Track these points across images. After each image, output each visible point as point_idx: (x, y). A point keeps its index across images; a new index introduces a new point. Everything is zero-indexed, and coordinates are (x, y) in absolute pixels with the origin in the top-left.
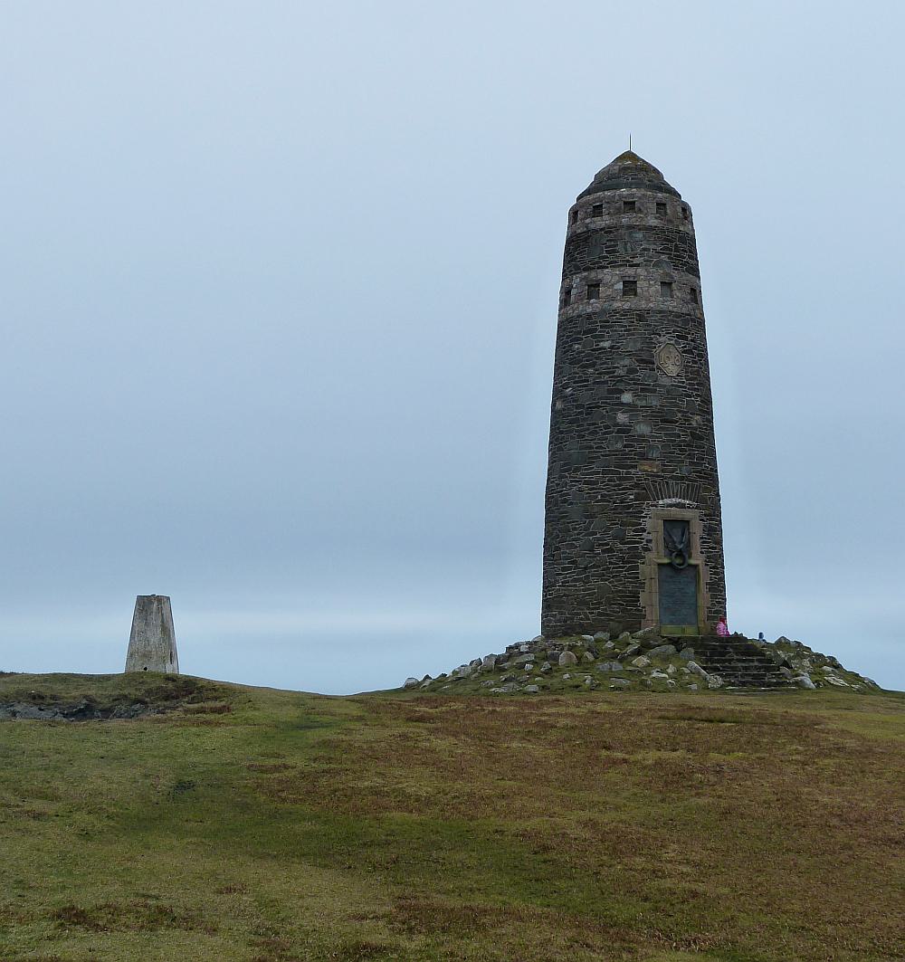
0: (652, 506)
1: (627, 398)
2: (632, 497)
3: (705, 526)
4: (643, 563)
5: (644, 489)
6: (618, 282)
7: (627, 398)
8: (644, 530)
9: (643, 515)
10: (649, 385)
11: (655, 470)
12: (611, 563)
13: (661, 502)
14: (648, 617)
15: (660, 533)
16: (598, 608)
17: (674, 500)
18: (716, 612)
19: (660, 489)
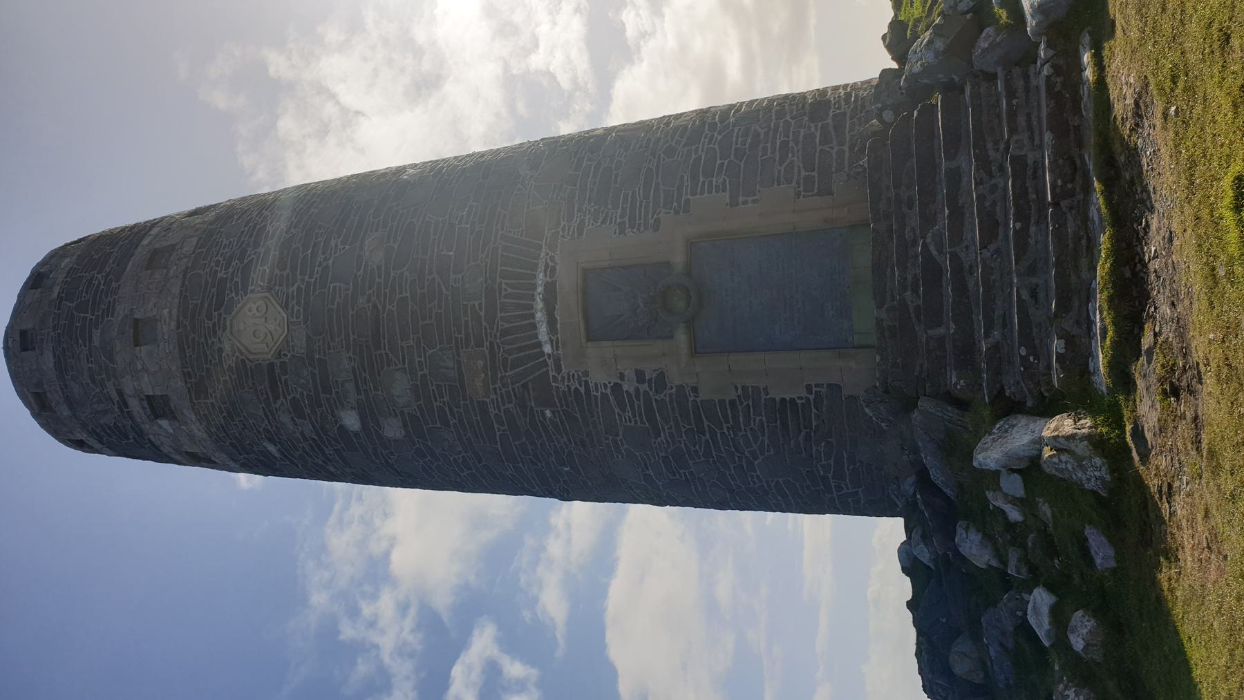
0: (559, 369)
1: (351, 421)
2: (548, 413)
4: (695, 390)
5: (525, 386)
6: (160, 427)
7: (351, 421)
8: (617, 388)
9: (582, 390)
10: (313, 375)
11: (480, 363)
13: (547, 349)
17: (539, 315)
19: (520, 349)
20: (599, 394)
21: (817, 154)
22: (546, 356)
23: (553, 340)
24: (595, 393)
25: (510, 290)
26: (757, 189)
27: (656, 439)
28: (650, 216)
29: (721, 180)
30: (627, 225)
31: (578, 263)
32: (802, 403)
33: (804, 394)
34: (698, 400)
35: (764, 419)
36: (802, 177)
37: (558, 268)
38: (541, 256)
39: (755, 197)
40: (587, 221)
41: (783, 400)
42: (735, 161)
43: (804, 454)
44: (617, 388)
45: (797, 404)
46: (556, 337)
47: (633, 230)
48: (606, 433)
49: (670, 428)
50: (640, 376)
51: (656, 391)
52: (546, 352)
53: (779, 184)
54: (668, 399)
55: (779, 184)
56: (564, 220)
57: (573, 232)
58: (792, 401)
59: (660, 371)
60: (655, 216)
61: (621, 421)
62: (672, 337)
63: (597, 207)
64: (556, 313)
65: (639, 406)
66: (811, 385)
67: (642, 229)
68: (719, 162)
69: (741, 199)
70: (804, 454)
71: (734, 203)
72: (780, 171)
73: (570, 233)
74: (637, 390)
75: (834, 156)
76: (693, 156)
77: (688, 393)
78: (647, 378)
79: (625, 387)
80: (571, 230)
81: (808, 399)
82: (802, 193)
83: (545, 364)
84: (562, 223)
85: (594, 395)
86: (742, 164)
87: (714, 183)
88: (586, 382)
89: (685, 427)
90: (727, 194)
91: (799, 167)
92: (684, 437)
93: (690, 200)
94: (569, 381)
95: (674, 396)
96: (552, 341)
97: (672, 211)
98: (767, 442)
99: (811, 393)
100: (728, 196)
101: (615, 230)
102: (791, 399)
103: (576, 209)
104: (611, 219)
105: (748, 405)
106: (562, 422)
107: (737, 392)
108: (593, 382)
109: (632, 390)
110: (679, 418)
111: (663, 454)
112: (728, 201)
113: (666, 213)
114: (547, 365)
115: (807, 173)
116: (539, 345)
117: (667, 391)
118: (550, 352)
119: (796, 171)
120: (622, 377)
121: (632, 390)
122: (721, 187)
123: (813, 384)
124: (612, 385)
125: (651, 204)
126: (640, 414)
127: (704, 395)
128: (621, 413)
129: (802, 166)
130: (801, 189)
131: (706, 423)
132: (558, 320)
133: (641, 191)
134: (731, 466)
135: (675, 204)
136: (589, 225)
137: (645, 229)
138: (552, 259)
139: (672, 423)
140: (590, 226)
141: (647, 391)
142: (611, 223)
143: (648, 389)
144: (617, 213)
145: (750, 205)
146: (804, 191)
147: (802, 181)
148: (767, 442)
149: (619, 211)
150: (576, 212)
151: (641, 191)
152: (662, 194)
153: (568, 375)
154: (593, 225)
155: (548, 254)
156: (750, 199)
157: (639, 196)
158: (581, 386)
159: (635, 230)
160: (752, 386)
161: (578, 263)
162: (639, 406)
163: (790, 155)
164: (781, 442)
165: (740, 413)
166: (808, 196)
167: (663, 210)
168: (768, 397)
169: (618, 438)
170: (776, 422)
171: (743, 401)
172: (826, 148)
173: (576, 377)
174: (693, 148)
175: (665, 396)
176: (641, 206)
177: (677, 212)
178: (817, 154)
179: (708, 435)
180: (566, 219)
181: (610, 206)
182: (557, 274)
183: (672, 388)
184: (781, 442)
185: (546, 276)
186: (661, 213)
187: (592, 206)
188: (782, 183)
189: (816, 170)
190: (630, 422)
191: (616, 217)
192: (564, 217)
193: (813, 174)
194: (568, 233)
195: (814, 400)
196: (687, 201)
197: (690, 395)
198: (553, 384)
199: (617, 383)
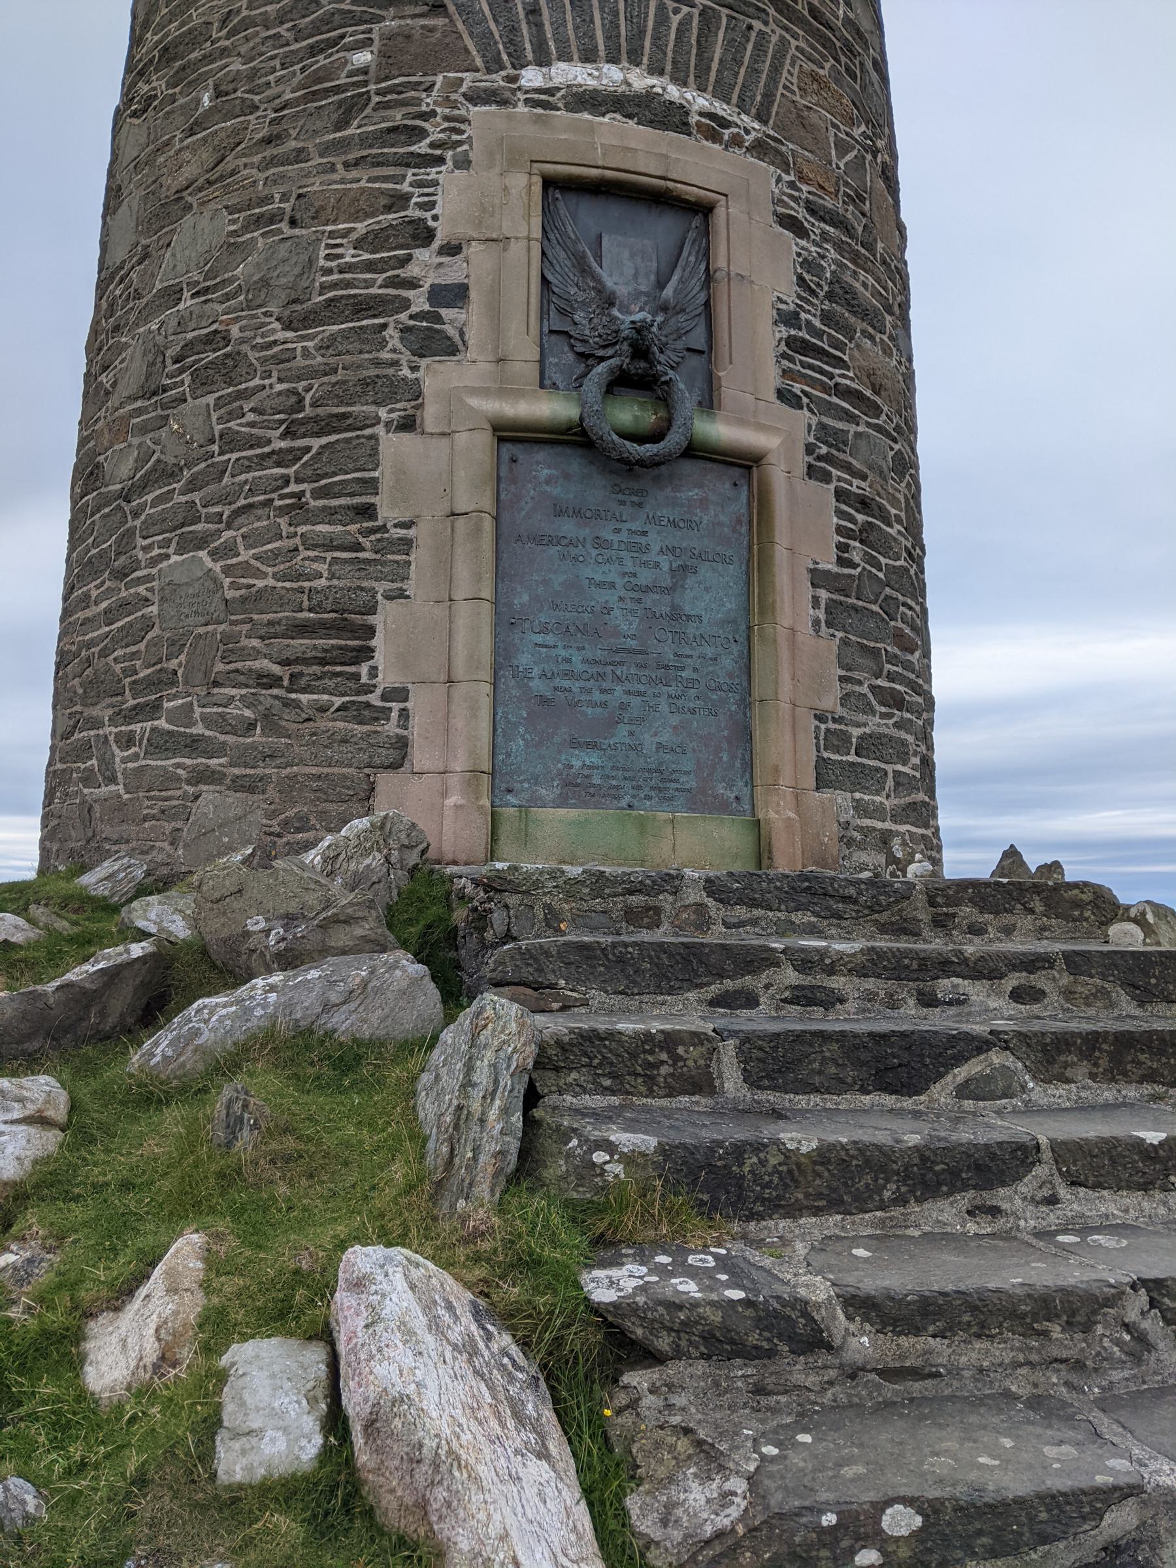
0: (474, 98)
2: (363, 58)
3: (807, 264)
4: (408, 425)
8: (425, 236)
9: (422, 147)
12: (230, 441)
13: (532, 77)
14: (420, 757)
15: (517, 249)
16: (154, 709)
18: (869, 745)
20: (405, 187)
21: (883, 766)
22: (511, 72)
23: (553, 95)
24: (409, 178)
25: (675, 20)
26: (836, 633)
27: (278, 319)
28: (807, 388)
29: (857, 559)
30: (793, 332)
31: (726, 196)
32: (356, 677)
33: (387, 679)
34: (380, 430)
35: (323, 582)
36: (850, 729)
37: (716, 146)
38: (743, 116)
39: (823, 624)
40: (803, 243)
41: (371, 631)
42: (882, 596)
43: (220, 667)
44: (425, 236)
45: (356, 662)
46: (560, 105)
47: (783, 343)
48: (300, 196)
49: (306, 353)
50: (457, 294)
51: (405, 330)
52: (523, 72)
53: (842, 679)
54: (386, 355)
55: (842, 679)
56: (809, 193)
57: (787, 206)
58: (366, 653)
59: (461, 347)
60: (805, 400)
61: (331, 235)
62: (542, 386)
63: (828, 275)
64: (618, 116)
65: (369, 284)
66: (406, 700)
67: (785, 363)
68: (883, 561)
69: (824, 594)
70: (220, 667)
71: (818, 578)
72: (860, 683)
73: (785, 198)
74: (413, 284)
75: (878, 799)
76: (893, 511)
77: (398, 406)
78: (443, 312)
79: (424, 255)
80: (792, 204)
81: (370, 689)
82: (823, 726)
83: (494, 65)
84: (805, 188)
85: (404, 176)
86: (876, 608)
87: (851, 542)
88: (441, 160)
89: (307, 390)
90: (832, 567)
91: (865, 725)
92: (279, 387)
93: (828, 483)
94: (447, 118)
95: (390, 371)
96: (550, 92)
97: (812, 440)
98: (260, 584)
99: (385, 697)
100: (830, 566)
101: (786, 303)
102: (372, 650)
103: (828, 228)
104: (808, 302)
105: (357, 547)
106: (338, 90)
107: (395, 526)
108: (441, 178)
109: (412, 270)
110: (334, 379)
111: (235, 331)
112: (820, 566)
113: (810, 426)
114: (489, 71)
115: (854, 740)
116: (543, 60)
117: (405, 357)
118: (523, 82)
119: (862, 718)
120: (452, 249)
121: (412, 270)
122: (846, 555)
123: (409, 705)
124: (430, 223)
125: (826, 396)
126: (348, 284)
127: (392, 445)
128: (354, 236)
129: (867, 730)
130: (832, 726)
131: (316, 443)
132: (600, 119)
133: (848, 382)
134: (196, 497)
135: (824, 450)
136: (797, 245)
137: (784, 370)
138: (736, 141)
139: (319, 359)
140: (795, 248)
141: (408, 308)
142: (799, 297)
143: (414, 309)
144: (814, 315)
145: (811, 611)
146: (828, 730)
147: (842, 727)
148: (260, 584)
149: (817, 323)
150: (822, 225)
151: (848, 382)
152: (840, 425)
153: (464, 120)
154: (799, 255)
155: (747, 132)
156: (822, 616)
157: (839, 376)
158: (432, 145)
159: (783, 347)
160: (409, 563)
161: (726, 196)
162: (369, 284)
163: (883, 710)
164: (256, 617)
165: (340, 528)
166: (817, 738)
167: (814, 421)
168: (379, 597)
169: (284, 226)
170: (310, 610)
171: (373, 538)
172: (890, 783)
173: (455, 137)
174: (903, 515)
175: (394, 351)
176: (822, 372)
177: (810, 449)
178: (883, 766)
179: (283, 444)
180: (811, 197)
181: (826, 306)
182: (705, 142)
183: (414, 369)
184: (256, 617)
185: (701, 114)
186: (808, 414)
187: (830, 265)
188: (844, 685)
189: (859, 760)
190: (328, 257)
191: (809, 312)
192: (815, 194)
193: (853, 751)
194: (784, 194)
195: (368, 705)
196: (826, 478)
197: (391, 411)
198: (439, 79)
199: (433, 236)
